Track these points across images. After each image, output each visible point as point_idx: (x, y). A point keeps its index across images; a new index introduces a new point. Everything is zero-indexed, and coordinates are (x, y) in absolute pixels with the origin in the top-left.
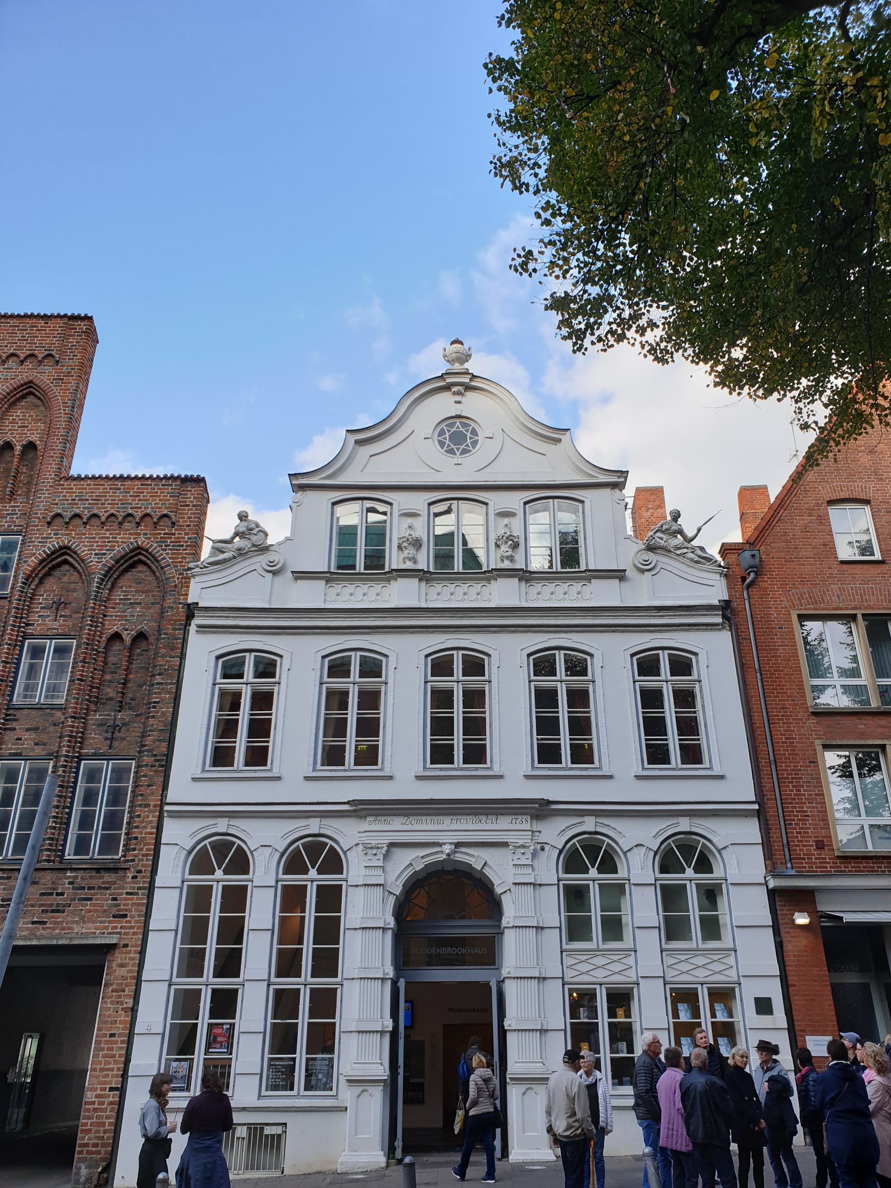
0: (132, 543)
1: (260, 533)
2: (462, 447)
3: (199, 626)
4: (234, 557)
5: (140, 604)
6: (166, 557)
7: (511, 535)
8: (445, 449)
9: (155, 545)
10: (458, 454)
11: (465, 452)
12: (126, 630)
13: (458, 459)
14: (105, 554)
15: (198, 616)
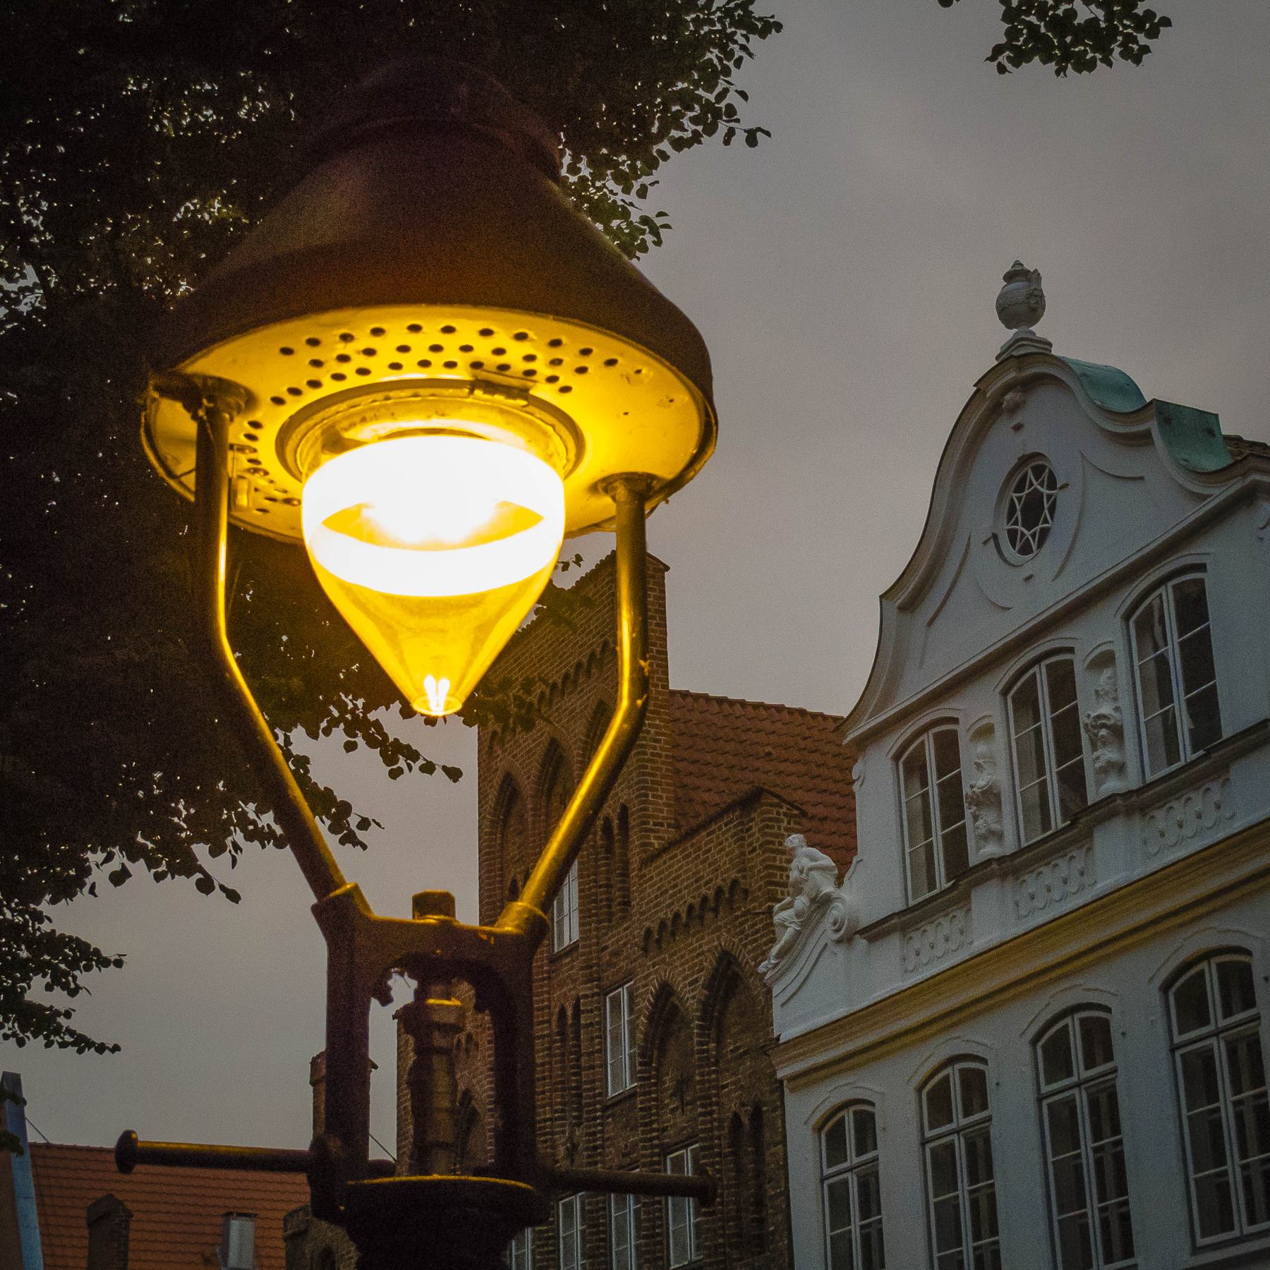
0: (716, 947)
1: (814, 873)
2: (1038, 528)
3: (793, 1078)
4: (798, 933)
5: (745, 1053)
6: (745, 957)
7: (1099, 717)
8: (1018, 546)
9: (736, 940)
10: (1034, 547)
11: (1044, 534)
12: (743, 1105)
13: (1031, 565)
14: (696, 980)
15: (780, 1063)
